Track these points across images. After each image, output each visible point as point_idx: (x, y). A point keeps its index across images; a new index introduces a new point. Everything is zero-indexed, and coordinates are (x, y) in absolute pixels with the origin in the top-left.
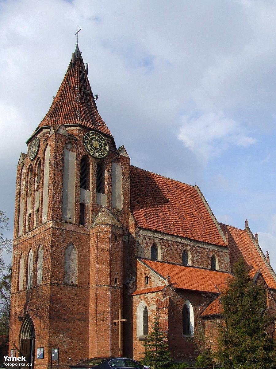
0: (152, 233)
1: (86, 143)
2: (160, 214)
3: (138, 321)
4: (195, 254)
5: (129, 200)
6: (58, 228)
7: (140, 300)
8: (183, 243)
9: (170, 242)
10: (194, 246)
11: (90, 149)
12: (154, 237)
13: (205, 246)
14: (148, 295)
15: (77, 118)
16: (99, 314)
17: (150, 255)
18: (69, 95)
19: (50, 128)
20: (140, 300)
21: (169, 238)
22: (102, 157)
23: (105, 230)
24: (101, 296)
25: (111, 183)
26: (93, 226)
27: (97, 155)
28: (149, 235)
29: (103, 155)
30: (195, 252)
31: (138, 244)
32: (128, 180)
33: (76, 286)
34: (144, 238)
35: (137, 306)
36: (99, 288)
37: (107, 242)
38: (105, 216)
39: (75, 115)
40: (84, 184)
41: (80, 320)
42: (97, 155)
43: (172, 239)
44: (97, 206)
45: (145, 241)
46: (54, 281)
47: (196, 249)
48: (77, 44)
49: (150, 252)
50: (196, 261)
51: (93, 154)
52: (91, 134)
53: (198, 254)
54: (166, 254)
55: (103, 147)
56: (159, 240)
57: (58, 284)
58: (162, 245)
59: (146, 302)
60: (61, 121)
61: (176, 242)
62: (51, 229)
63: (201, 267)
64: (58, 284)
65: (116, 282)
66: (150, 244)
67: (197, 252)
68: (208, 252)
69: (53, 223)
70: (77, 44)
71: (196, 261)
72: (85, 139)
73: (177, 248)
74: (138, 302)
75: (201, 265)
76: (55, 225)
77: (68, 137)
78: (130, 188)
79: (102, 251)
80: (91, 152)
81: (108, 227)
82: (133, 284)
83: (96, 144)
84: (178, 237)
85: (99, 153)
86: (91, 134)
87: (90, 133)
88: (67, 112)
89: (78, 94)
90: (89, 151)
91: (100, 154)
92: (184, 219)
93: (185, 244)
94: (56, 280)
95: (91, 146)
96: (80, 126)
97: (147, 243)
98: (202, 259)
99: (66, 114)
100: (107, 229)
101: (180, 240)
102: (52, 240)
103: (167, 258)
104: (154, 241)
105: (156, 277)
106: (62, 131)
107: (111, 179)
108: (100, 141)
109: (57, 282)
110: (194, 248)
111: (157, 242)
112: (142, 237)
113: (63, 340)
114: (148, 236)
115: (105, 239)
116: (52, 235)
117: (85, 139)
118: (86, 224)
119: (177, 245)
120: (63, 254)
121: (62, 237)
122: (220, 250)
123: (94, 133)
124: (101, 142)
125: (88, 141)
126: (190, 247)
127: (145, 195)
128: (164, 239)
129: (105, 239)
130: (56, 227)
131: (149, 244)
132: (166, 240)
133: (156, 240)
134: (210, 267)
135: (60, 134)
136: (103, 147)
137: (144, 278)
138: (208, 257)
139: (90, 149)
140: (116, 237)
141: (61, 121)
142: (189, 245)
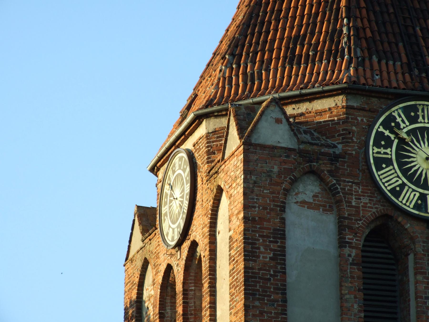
1: (380, 163)
11: (403, 185)
15: (335, 53)
39: (334, 35)
52: (400, 118)
72: (377, 144)
77: (301, 153)
80: (408, 199)
86: (400, 118)
87: (397, 111)
88: (300, 26)
90: (396, 193)
95: (405, 172)
96: (350, 90)
99: (297, 36)
106: (273, 133)
117: (377, 144)
123: (414, 108)
125: (392, 153)
135: (263, 147)
139: (403, 185)
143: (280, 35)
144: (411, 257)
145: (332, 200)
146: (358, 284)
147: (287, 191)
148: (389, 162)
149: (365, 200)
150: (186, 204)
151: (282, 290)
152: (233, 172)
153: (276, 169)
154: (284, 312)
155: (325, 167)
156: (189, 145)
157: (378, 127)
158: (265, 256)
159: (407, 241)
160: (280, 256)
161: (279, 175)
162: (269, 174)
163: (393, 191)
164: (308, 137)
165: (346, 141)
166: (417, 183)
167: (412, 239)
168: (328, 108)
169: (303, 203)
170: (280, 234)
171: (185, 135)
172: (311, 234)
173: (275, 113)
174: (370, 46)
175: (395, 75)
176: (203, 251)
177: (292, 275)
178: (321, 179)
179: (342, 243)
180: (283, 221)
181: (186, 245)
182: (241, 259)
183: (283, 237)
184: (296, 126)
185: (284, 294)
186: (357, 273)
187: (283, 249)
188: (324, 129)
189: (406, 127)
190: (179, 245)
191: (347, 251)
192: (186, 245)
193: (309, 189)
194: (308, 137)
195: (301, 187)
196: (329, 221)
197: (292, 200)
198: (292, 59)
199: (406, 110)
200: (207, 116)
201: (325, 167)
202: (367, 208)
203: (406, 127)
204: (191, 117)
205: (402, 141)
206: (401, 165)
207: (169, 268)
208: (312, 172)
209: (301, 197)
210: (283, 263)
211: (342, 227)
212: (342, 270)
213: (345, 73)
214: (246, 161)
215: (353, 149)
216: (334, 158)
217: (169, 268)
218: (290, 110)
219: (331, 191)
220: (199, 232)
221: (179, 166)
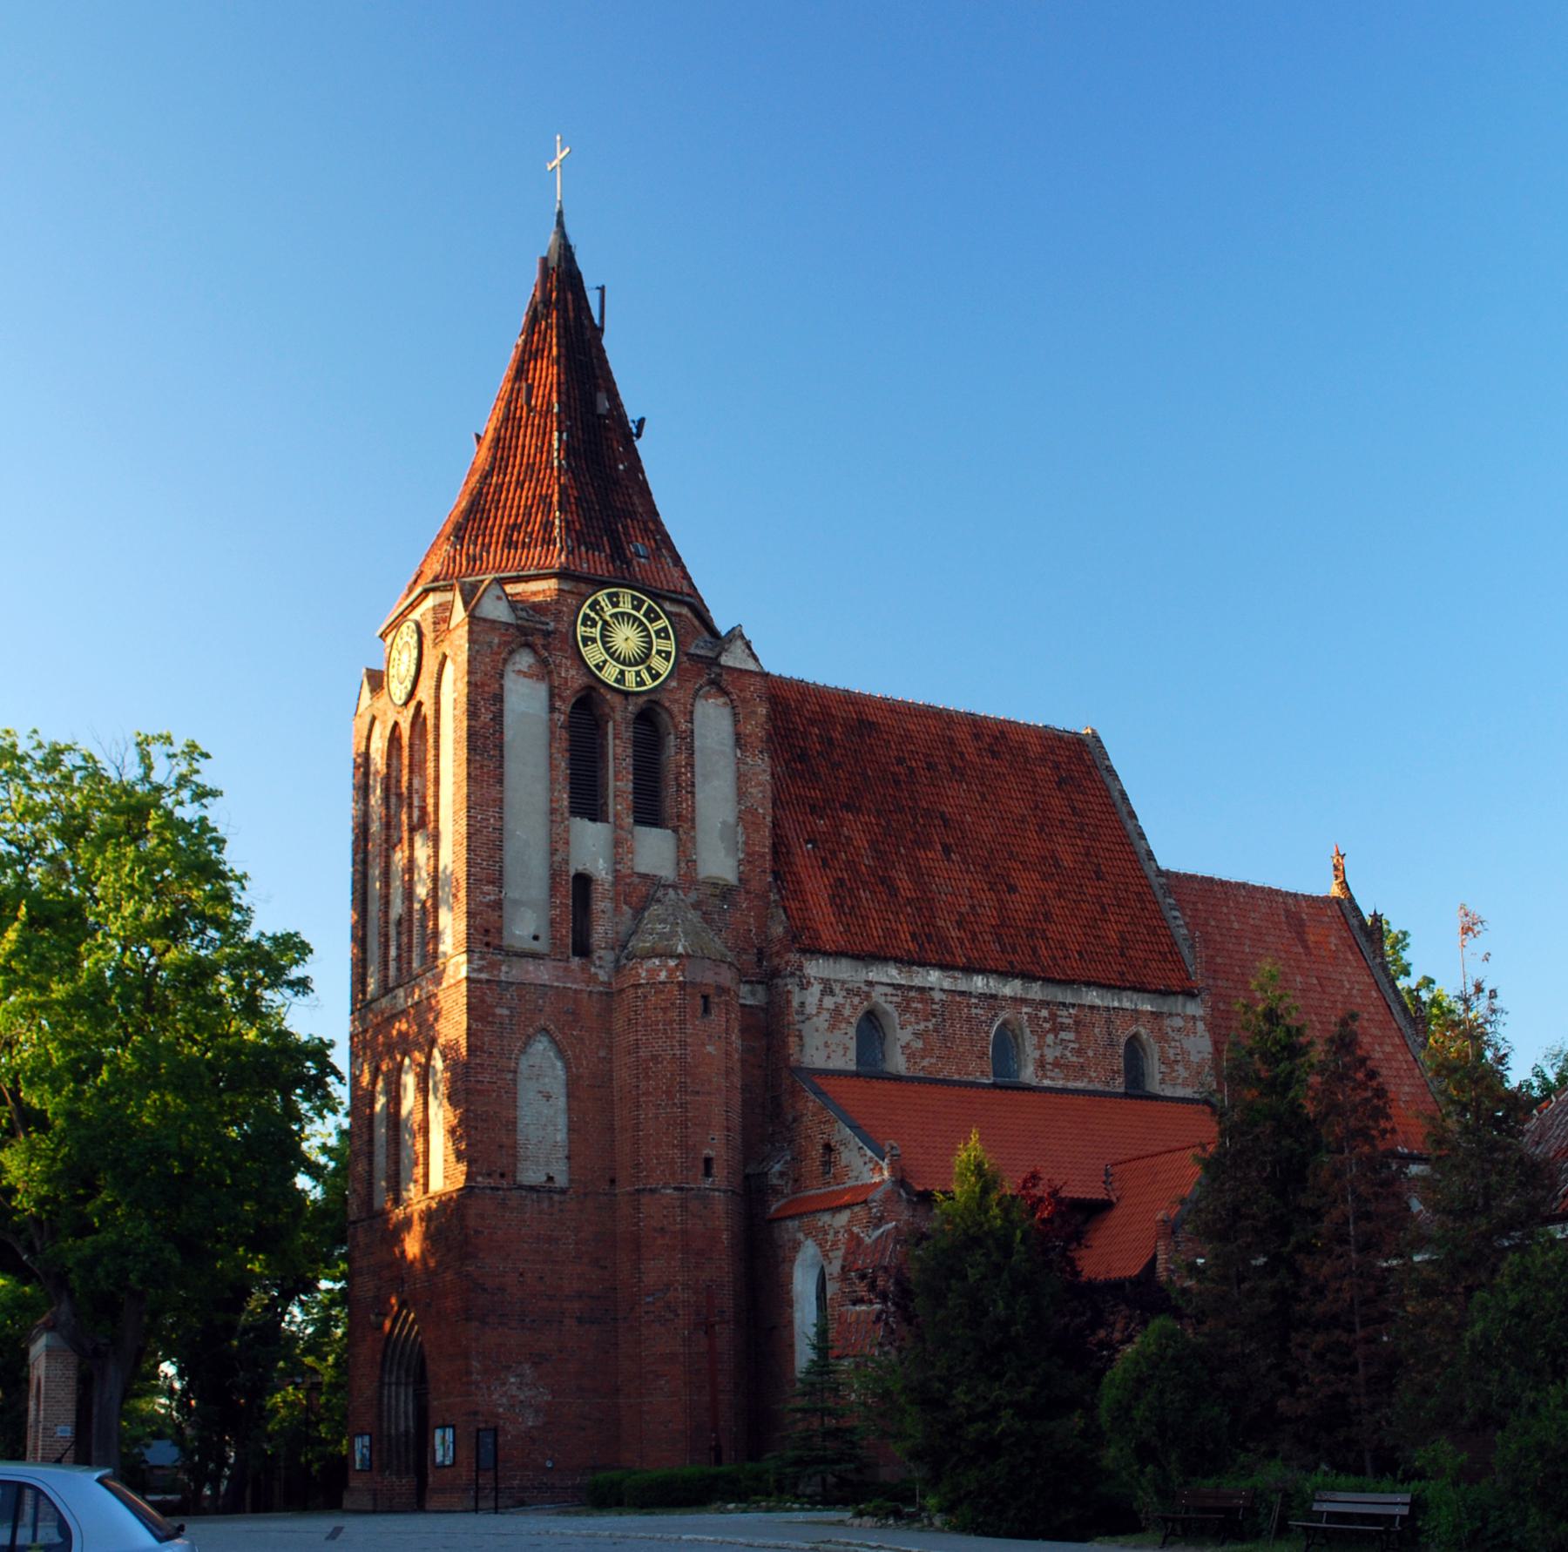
0: (860, 964)
1: (586, 640)
2: (904, 883)
3: (797, 1316)
4: (1050, 1038)
5: (768, 842)
6: (488, 981)
7: (801, 1236)
8: (994, 997)
9: (937, 996)
10: (1045, 1004)
11: (605, 662)
12: (870, 984)
13: (1092, 997)
14: (826, 1218)
15: (548, 541)
16: (648, 1295)
17: (852, 1054)
18: (528, 440)
19: (451, 588)
20: (801, 1236)
21: (934, 977)
22: (650, 684)
23: (663, 976)
24: (655, 1230)
25: (693, 785)
26: (624, 961)
27: (630, 677)
28: (844, 976)
29: (655, 677)
30: (1047, 1026)
31: (801, 1018)
32: (761, 767)
33: (563, 1191)
34: (828, 990)
35: (792, 1261)
36: (645, 1199)
37: (672, 1021)
38: (664, 921)
39: (548, 526)
40: (586, 799)
41: (580, 1321)
42: (630, 682)
43: (946, 985)
44: (636, 880)
45: (829, 1002)
46: (479, 1179)
47: (1053, 1016)
48: (560, 214)
49: (853, 1044)
50: (1056, 1064)
51: (617, 681)
53: (1063, 1035)
54: (919, 1044)
55: (658, 644)
56: (889, 990)
57: (498, 1189)
58: (904, 1007)
59: (820, 1245)
60: (494, 556)
61: (962, 993)
62: (464, 985)
63: (1080, 1085)
64: (498, 1189)
65: (708, 1173)
66: (853, 1011)
67: (1057, 1028)
68: (1109, 1021)
69: (469, 961)
70: (560, 214)
71: (1056, 1064)
72: (584, 624)
73: (969, 1019)
74: (797, 1246)
75: (1076, 1079)
76: (480, 970)
77: (518, 627)
78: (769, 794)
79: (655, 1058)
80: (610, 674)
81: (672, 963)
82: (782, 1174)
83: (626, 639)
84: (969, 970)
85: (638, 674)
87: (601, 596)
88: (517, 515)
89: (560, 434)
90: (600, 668)
91: (645, 675)
92: (1012, 889)
93: (1004, 998)
94: (489, 1175)
95: (607, 650)
96: (561, 575)
97: (837, 1011)
98: (1079, 1052)
99: (515, 525)
100: (671, 972)
101: (979, 983)
102: (469, 1028)
103: (925, 1063)
104: (868, 996)
105: (855, 1151)
106: (495, 610)
107: (692, 766)
108: (641, 623)
109: (491, 1182)
110: (1044, 1013)
111: (881, 1000)
112: (816, 989)
113: (522, 1397)
114: (843, 982)
115: (665, 1010)
116: (471, 1009)
118: (595, 956)
119: (969, 1006)
120: (510, 1076)
121: (505, 1012)
122: (1165, 1009)
123: (616, 595)
124: (646, 629)
125: (596, 632)
126: (1025, 1010)
127: (847, 807)
128: (911, 988)
129: (665, 1010)
130: (484, 976)
131: (847, 1012)
132: (921, 990)
133: (877, 994)
134: (1119, 1085)
135: (485, 620)
136: (658, 644)
137: (817, 1152)
138: (1111, 1044)
139: (605, 662)
140: (705, 998)
141: (494, 556)
142: (1024, 1001)
143: (499, 522)
144: (611, 724)
145: (544, 670)
146: (565, 745)
147: (505, 661)
148: (594, 640)
149: (573, 672)
150: (413, 668)
151: (500, 747)
152: (458, 644)
153: (496, 641)
154: (501, 766)
155: (538, 641)
156: (416, 615)
157: (585, 609)
158: (486, 717)
159: (607, 710)
160: (498, 717)
161: (499, 645)
162: (490, 644)
163: (597, 666)
164: (524, 614)
165: (557, 619)
166: (617, 660)
167: (613, 709)
168: (543, 589)
169: (519, 672)
170: (499, 698)
171: (413, 606)
172: (526, 700)
173: (496, 590)
174: (579, 537)
175: (597, 563)
176: (428, 710)
177: (509, 735)
178: (535, 652)
179: (552, 709)
180: (502, 686)
181: (413, 704)
182: (464, 718)
183: (502, 701)
184: (514, 604)
185: (501, 751)
186: (565, 735)
187: (501, 711)
188: (538, 608)
189: (609, 611)
190: (406, 704)
191: (556, 715)
192: (413, 704)
193: (524, 660)
194: (524, 614)
195: (517, 657)
196: (542, 689)
197: (509, 668)
198: (510, 544)
199: (610, 596)
200: (434, 590)
201: (538, 641)
202: (576, 680)
203: (609, 611)
204: (418, 590)
205: (605, 623)
206: (604, 643)
207: (396, 724)
208: (528, 645)
209: (518, 667)
210: (501, 724)
211: (552, 695)
212: (552, 733)
213: (558, 560)
214: (470, 632)
215: (563, 628)
216: (547, 634)
217: (396, 724)
218: (509, 589)
219: (544, 662)
220: (425, 693)
221: (407, 633)
